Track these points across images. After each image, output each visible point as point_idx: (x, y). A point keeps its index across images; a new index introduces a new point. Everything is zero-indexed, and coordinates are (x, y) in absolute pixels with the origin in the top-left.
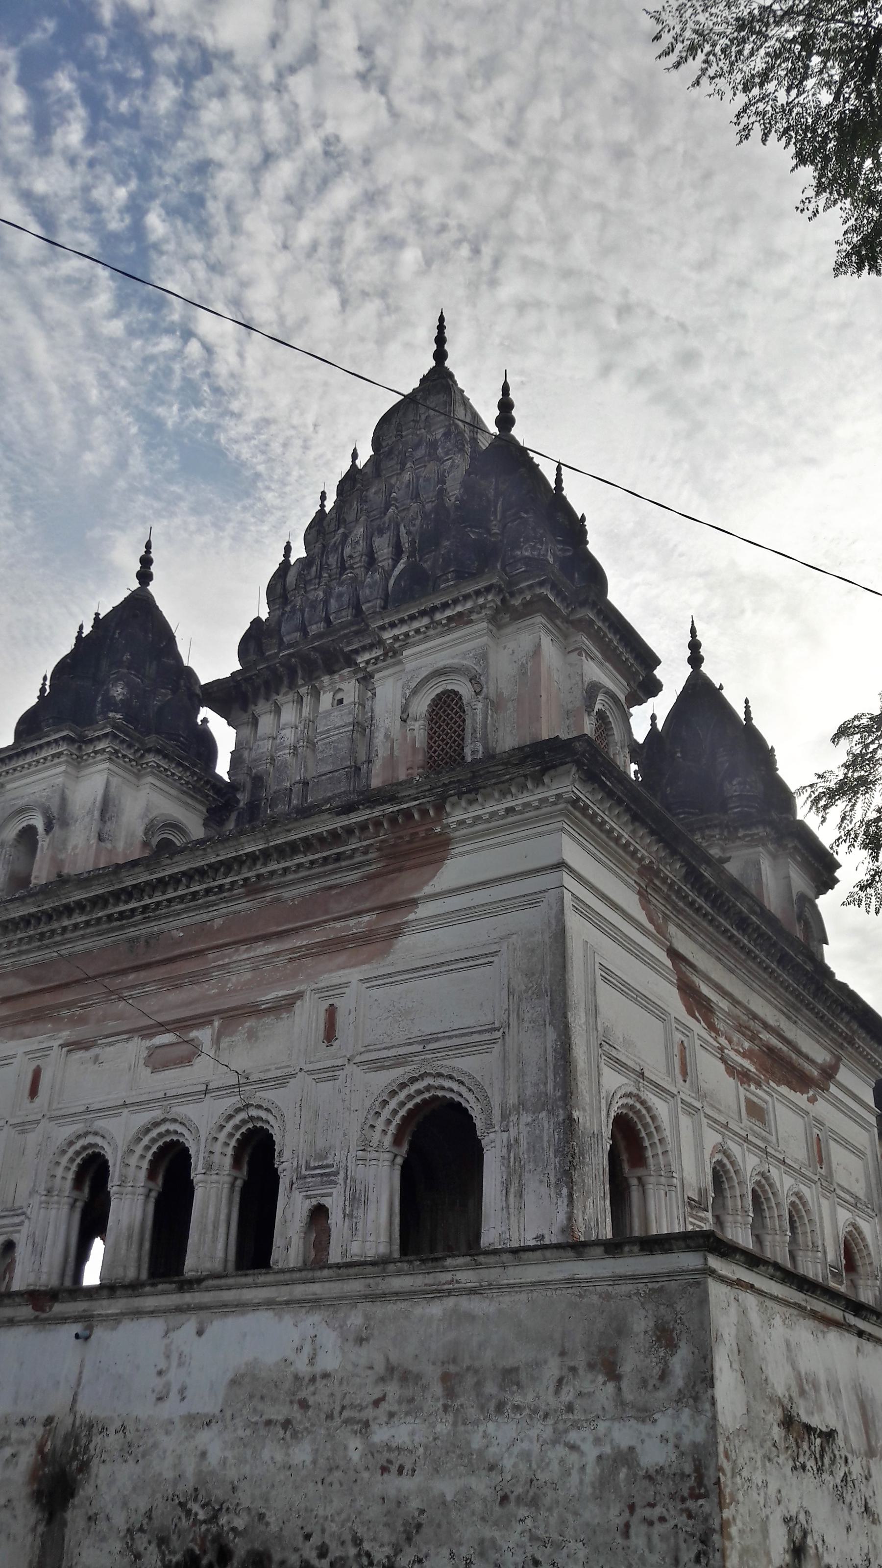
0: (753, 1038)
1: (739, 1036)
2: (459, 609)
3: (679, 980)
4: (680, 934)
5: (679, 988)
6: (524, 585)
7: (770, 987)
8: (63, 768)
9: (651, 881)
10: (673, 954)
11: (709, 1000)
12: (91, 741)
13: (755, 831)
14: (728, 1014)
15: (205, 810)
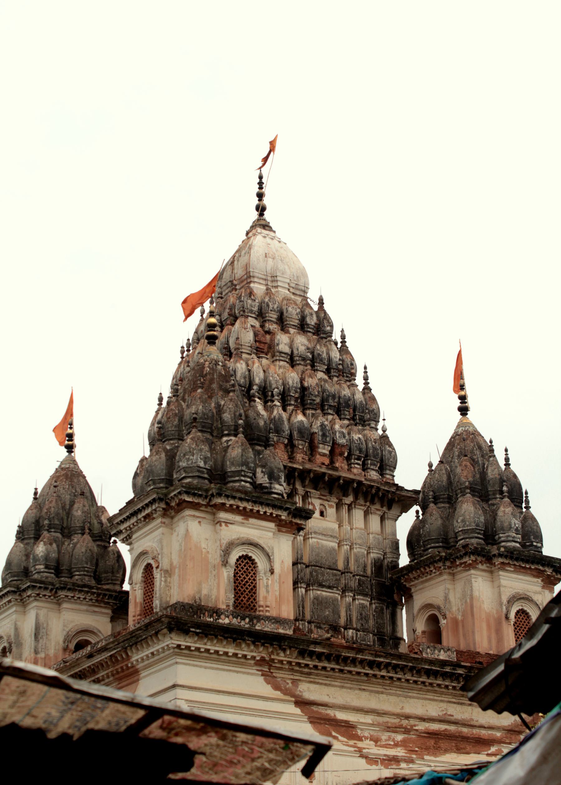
0: (407, 731)
1: (389, 734)
2: (147, 511)
3: (309, 718)
4: (312, 687)
5: (311, 722)
6: (172, 494)
7: (428, 691)
8: (14, 609)
9: (271, 666)
10: (301, 703)
11: (346, 722)
12: (24, 590)
13: (464, 560)
14: (373, 724)
15: (109, 611)
